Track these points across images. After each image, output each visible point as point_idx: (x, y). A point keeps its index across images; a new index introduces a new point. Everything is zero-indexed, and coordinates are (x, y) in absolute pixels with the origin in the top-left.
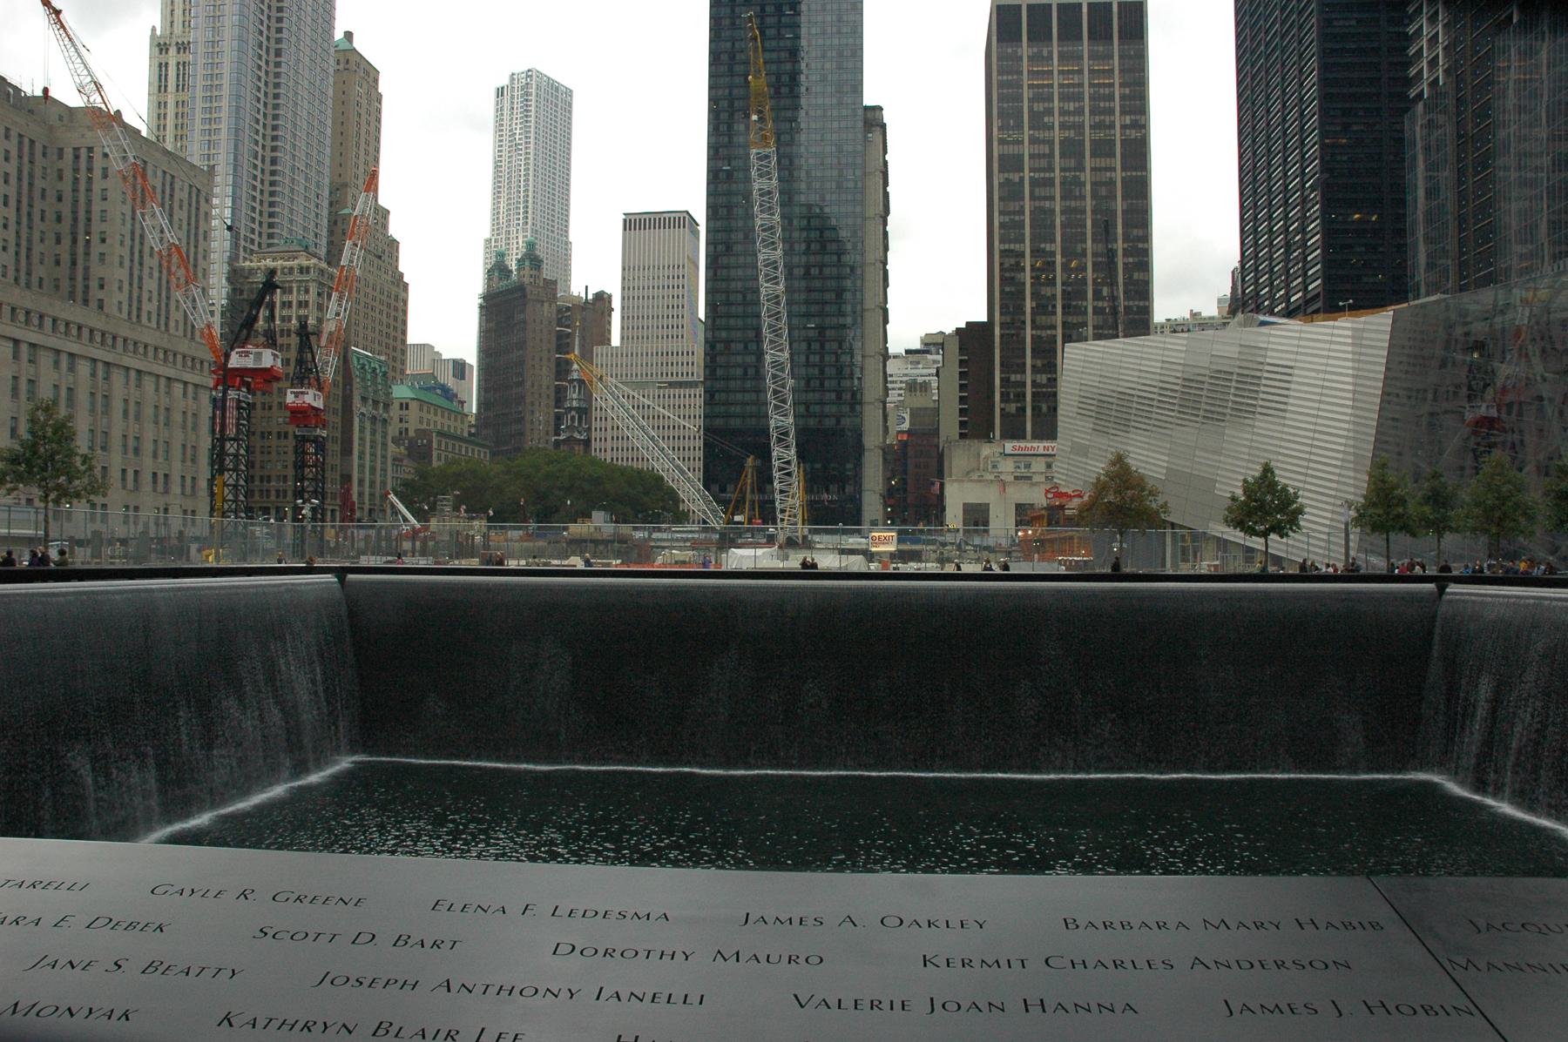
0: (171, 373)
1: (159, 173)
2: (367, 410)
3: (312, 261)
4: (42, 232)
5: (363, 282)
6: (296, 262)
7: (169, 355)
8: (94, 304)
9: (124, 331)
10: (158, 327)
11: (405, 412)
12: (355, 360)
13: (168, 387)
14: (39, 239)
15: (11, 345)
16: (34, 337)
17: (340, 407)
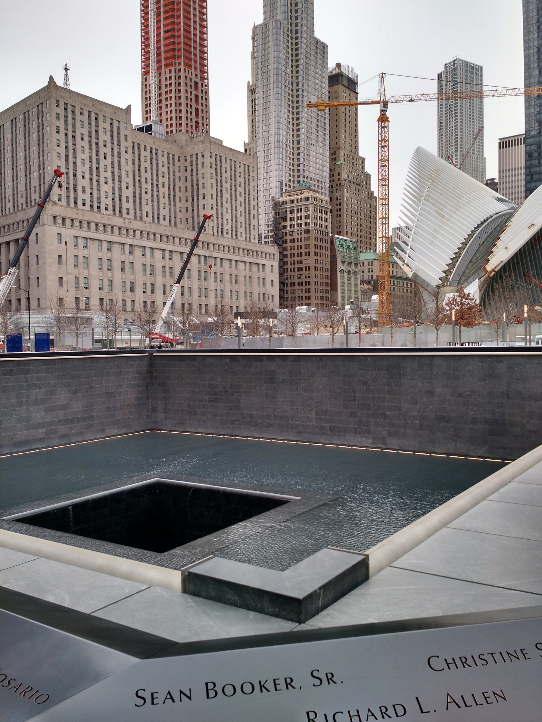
0: (237, 258)
1: (228, 161)
2: (345, 267)
3: (310, 194)
4: (180, 197)
6: (303, 195)
7: (236, 249)
9: (213, 240)
10: (232, 237)
12: (338, 243)
13: (236, 265)
14: (179, 201)
15: (161, 252)
16: (171, 248)
17: (329, 267)
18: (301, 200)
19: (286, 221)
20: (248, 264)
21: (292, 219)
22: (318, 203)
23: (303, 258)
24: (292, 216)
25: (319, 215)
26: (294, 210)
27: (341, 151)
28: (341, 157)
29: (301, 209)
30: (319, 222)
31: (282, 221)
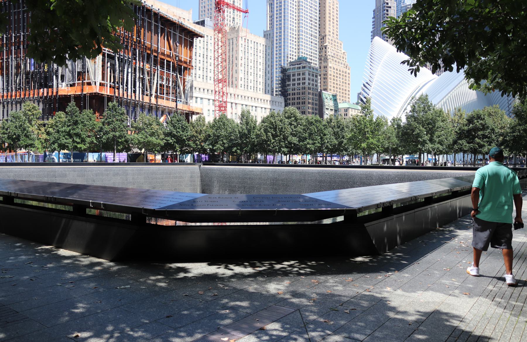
1: (253, 42)
5: (332, 68)
8: (234, 86)
9: (241, 94)
11: (346, 113)
18: (300, 68)
19: (290, 81)
20: (263, 109)
21: (294, 80)
22: (311, 70)
23: (301, 105)
24: (294, 78)
25: (311, 77)
26: (295, 74)
27: (327, 37)
28: (327, 40)
29: (300, 74)
30: (311, 82)
31: (287, 81)
